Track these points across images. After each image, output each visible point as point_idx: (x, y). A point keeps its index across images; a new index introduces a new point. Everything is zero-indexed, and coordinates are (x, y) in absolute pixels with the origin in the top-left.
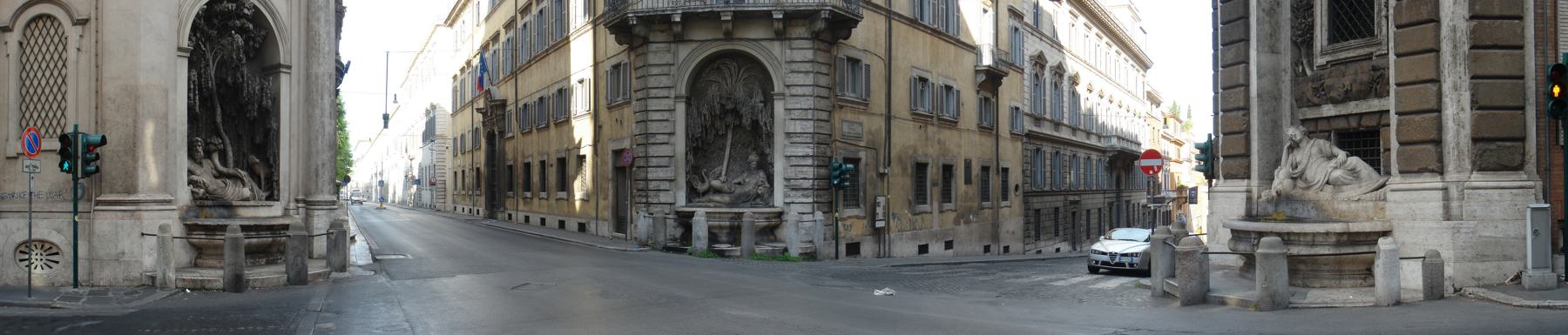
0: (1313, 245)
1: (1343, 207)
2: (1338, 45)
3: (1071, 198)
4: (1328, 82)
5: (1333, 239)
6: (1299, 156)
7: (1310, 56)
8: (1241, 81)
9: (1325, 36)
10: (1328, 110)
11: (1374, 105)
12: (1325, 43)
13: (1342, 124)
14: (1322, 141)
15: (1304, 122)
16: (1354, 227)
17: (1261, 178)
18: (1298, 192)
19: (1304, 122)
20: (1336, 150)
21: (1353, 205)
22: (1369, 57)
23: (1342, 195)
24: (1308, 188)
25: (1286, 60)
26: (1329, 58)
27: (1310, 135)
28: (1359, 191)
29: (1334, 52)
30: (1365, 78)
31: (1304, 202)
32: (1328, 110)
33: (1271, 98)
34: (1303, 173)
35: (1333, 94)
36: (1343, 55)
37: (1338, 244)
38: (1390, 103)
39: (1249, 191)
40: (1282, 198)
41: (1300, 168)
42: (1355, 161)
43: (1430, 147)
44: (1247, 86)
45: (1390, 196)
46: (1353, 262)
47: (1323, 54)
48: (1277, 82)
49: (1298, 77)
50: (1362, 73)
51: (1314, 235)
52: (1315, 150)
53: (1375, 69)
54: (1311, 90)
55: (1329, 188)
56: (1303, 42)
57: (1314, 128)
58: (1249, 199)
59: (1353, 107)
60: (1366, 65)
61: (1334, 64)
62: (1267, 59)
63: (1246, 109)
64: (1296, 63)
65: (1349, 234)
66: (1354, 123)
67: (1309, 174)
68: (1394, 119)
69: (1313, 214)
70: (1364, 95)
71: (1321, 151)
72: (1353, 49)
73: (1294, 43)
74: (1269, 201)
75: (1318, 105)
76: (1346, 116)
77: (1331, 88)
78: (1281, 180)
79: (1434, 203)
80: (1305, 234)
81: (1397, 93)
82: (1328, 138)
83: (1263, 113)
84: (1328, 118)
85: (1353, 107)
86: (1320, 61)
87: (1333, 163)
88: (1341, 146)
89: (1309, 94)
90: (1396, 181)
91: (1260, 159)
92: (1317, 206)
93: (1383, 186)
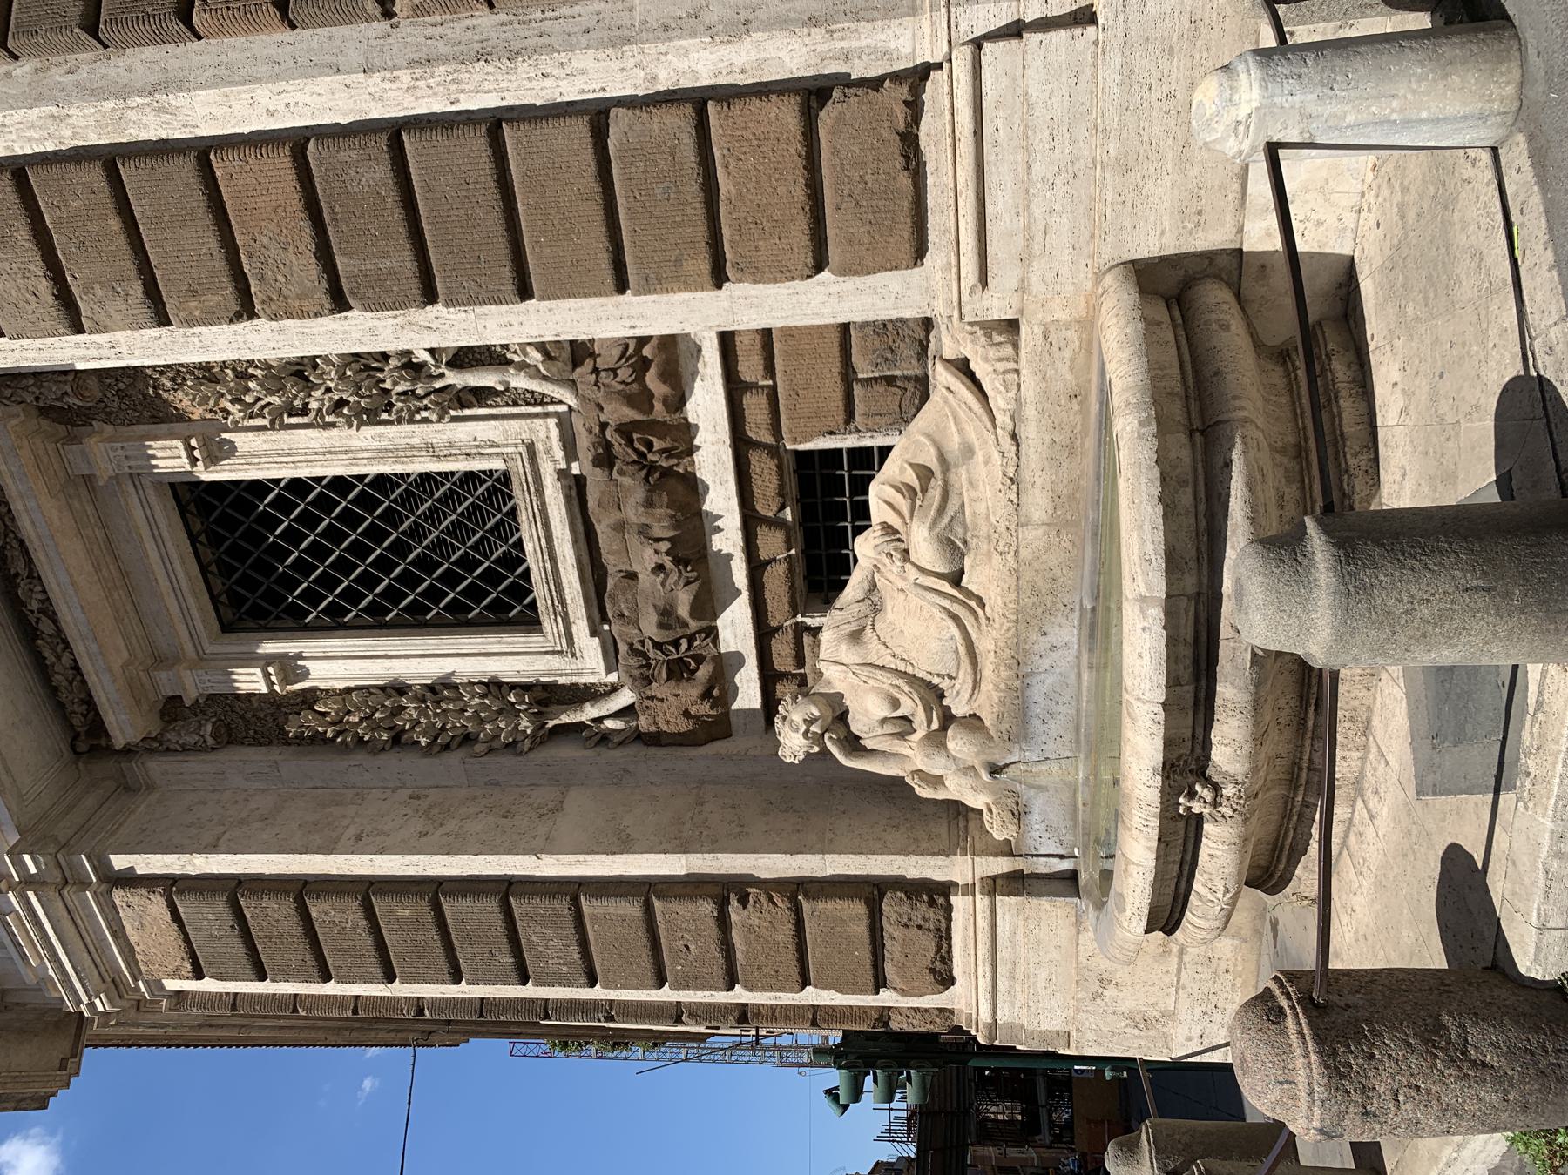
2: (540, 592)
4: (650, 626)
6: (867, 712)
8: (633, 909)
9: (517, 641)
10: (735, 627)
12: (534, 641)
26: (581, 628)
30: (632, 487)
32: (735, 627)
43: (826, 118)
44: (647, 889)
53: (605, 459)
61: (598, 614)
63: (726, 891)
77: (667, 616)
79: (1031, 74)
86: (589, 664)
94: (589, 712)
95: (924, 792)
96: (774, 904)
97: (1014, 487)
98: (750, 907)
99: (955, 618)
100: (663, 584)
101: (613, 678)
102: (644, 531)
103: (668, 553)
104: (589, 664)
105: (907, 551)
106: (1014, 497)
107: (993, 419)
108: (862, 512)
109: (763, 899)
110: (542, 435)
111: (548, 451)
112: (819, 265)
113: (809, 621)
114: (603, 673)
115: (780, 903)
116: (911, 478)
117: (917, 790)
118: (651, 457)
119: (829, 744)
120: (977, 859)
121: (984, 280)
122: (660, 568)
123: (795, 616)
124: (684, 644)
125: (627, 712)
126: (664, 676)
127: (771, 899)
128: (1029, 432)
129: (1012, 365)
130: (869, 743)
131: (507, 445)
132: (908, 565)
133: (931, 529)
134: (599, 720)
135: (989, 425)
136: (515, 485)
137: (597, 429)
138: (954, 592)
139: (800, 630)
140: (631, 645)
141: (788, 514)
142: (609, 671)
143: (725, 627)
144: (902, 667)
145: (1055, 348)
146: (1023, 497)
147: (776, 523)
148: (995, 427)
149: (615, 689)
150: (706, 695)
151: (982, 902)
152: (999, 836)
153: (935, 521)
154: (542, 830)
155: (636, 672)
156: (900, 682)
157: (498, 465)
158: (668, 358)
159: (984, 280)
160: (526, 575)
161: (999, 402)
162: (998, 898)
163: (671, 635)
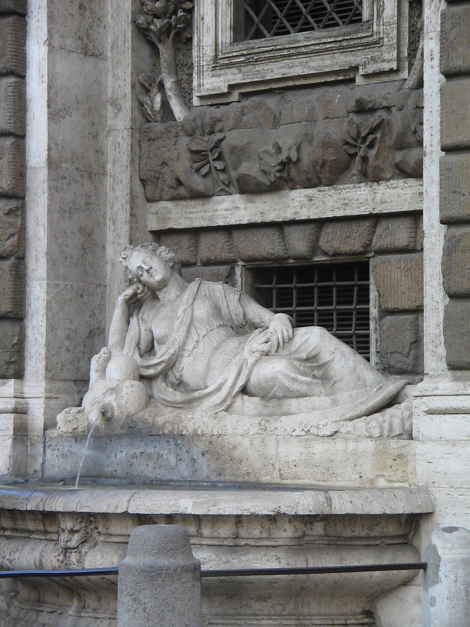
0: (235, 547)
1: (292, 451)
3: (158, 572)
4: (233, 138)
5: (286, 533)
7: (183, 69)
9: (226, 19)
10: (232, 209)
11: (393, 195)
12: (226, 36)
13: (267, 246)
14: (218, 288)
15: (160, 235)
16: (342, 505)
17: (52, 376)
18: (164, 417)
19: (160, 235)
20: (256, 311)
21: (319, 448)
22: (345, 78)
23: (285, 424)
24: (190, 403)
25: (119, 76)
27: (183, 268)
28: (335, 413)
29: (252, 59)
30: (338, 131)
31: (177, 438)
32: (232, 209)
33: (78, 169)
34: (171, 364)
35: (249, 168)
36: (275, 70)
37: (299, 545)
38: (428, 195)
39: (20, 411)
40: (113, 430)
41: (163, 353)
42: (314, 337)
44: (19, 135)
45: (423, 425)
46: (335, 592)
47: (219, 64)
48: (95, 132)
49: (150, 124)
50: (329, 120)
51: (238, 519)
52: (202, 310)
53: (362, 108)
54: (188, 156)
55: (249, 404)
56: (167, 30)
57: (195, 254)
58: (21, 433)
59: (297, 203)
60: (339, 97)
62: (72, 67)
64: (145, 85)
65: (327, 519)
66: (298, 243)
67: (189, 369)
68: (434, 236)
69: (205, 468)
70: (329, 173)
71: (217, 311)
72: (304, 55)
73: (142, 32)
74: (77, 437)
75: (202, 196)
76: (279, 226)
77: (241, 153)
78: (112, 381)
80: (216, 519)
81: (445, 171)
82: (229, 279)
83: (60, 211)
84: (228, 230)
85: (297, 203)
86: (210, 82)
87: (256, 342)
88: (265, 300)
89: (182, 166)
90: (437, 383)
91: (51, 329)
92: (214, 448)
93: (392, 401)
95: (95, 363)
96: (9, 238)
97: (303, 433)
98: (6, 218)
99: (218, 389)
100: (266, 152)
101: (196, 102)
102: (308, 138)
103: (289, 158)
105: (267, 355)
106: (297, 433)
107: (351, 419)
108: (301, 320)
109: (12, 230)
110: (386, 56)
111: (373, 59)
112: (453, 296)
113: (238, 271)
114: (199, 94)
115: (9, 243)
117: (96, 357)
118: (363, 147)
119: (134, 287)
120: (42, 401)
121: (431, 412)
122: (279, 150)
123: (242, 260)
124: (219, 165)
127: (13, 235)
128: (339, 445)
129: (386, 433)
130: (134, 321)
131: (378, 25)
132: (258, 355)
133: (280, 372)
134: (161, 87)
135: (347, 416)
136: (350, 28)
137: (385, 104)
138: (237, 388)
139: (231, 263)
140: (219, 120)
141: (319, 258)
142: (201, 98)
143: (233, 202)
144: (189, 347)
145: (391, 462)
146: (296, 439)
147: (315, 248)
148: (346, 420)
149: (186, 101)
150: (180, 183)
151: (10, 404)
152: (60, 417)
153: (286, 376)
154: (70, 42)
155: (199, 123)
156: (176, 347)
157: (366, 15)
158: (416, 173)
159: (431, 412)
160: (282, 31)
161: (360, 423)
162: (12, 416)
163: (226, 155)
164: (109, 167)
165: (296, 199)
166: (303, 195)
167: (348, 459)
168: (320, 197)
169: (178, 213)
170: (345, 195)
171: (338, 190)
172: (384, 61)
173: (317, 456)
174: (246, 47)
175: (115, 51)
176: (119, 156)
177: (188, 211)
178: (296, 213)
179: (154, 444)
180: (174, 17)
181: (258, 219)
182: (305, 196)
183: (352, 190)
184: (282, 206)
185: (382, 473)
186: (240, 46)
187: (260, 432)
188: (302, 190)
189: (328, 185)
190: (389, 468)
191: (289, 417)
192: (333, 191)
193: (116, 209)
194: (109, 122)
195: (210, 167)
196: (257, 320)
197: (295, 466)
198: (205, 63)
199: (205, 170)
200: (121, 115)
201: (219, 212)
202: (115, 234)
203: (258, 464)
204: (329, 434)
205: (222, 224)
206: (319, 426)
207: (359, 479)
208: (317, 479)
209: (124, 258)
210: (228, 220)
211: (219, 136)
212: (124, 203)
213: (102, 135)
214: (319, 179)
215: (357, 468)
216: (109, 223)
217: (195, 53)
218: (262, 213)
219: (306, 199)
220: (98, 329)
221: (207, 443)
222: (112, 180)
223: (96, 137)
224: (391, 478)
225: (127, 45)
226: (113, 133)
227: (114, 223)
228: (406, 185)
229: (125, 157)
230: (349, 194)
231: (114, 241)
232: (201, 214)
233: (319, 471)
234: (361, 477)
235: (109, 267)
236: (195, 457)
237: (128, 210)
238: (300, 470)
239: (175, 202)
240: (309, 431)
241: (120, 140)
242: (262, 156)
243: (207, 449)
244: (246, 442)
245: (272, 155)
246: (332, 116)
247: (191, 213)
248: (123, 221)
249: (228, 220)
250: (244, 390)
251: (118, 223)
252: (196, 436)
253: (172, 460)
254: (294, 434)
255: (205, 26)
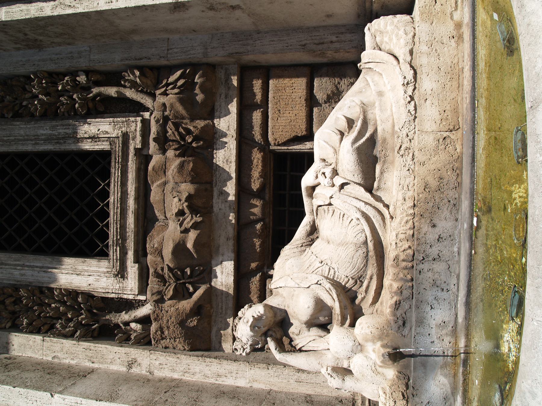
21: (427, 84)
26: (130, 255)
94: (125, 316)
101: (142, 298)
104: (130, 287)
110: (133, 128)
116: (343, 125)
122: (181, 213)
125: (145, 321)
126: (171, 293)
134: (127, 324)
140: (156, 272)
149: (142, 304)
164: (176, 376)
165: (220, 207)
166: (217, 201)
167: (436, 50)
168: (220, 184)
169: (221, 321)
170: (221, 162)
171: (217, 168)
172: (136, 130)
173: (435, 86)
174: (112, 247)
175: (95, 360)
176: (169, 364)
177: (220, 311)
178: (230, 207)
179: (422, 291)
180: (82, 305)
181: (231, 243)
182: (219, 199)
183: (218, 156)
184: (224, 220)
185: (448, 14)
186: (111, 253)
187: (411, 155)
188: (214, 201)
189: (212, 176)
190: (443, 7)
191: (395, 121)
192: (217, 173)
193: (209, 372)
194: (144, 372)
195: (189, 283)
196: (308, 228)
197: (444, 111)
198: (118, 285)
199: (191, 289)
200: (139, 360)
201: (223, 280)
202: (229, 375)
203: (443, 157)
204: (412, 72)
205: (233, 278)
206: (405, 83)
207: (456, 38)
208: (457, 86)
209: (244, 349)
210: (230, 272)
211: (166, 270)
212: (206, 364)
213: (150, 377)
214: (207, 183)
215: (445, 41)
216: (220, 381)
217: (113, 296)
218: (227, 239)
219: (221, 198)
220: (305, 397)
221: (423, 220)
222: (186, 375)
223: (149, 380)
224: (454, 5)
225: (92, 348)
226: (152, 369)
227: (219, 376)
228: (219, 110)
229: (171, 359)
230: (221, 159)
231: (234, 378)
232: (224, 298)
233: (449, 84)
234: (454, 38)
235: (256, 386)
236: (437, 237)
237: (211, 360)
238: (449, 106)
239: (213, 323)
240: (410, 96)
241: (157, 363)
242: (183, 228)
243: (428, 222)
244: (421, 171)
245: (184, 220)
246: (164, 167)
247: (222, 309)
248: (219, 366)
249: (230, 272)
250: (369, 189)
251: (222, 371)
252: (414, 236)
253: (440, 267)
254: (413, 113)
255: (94, 283)
